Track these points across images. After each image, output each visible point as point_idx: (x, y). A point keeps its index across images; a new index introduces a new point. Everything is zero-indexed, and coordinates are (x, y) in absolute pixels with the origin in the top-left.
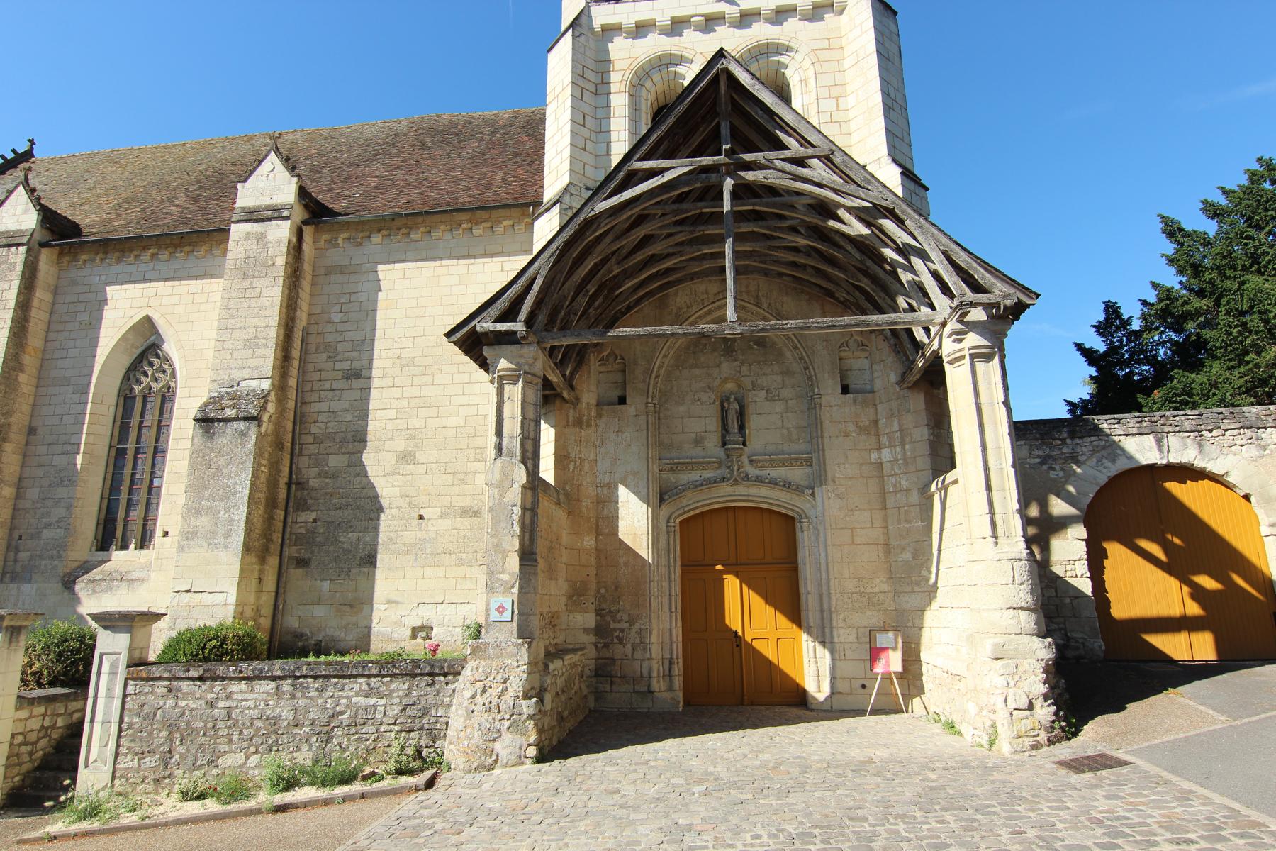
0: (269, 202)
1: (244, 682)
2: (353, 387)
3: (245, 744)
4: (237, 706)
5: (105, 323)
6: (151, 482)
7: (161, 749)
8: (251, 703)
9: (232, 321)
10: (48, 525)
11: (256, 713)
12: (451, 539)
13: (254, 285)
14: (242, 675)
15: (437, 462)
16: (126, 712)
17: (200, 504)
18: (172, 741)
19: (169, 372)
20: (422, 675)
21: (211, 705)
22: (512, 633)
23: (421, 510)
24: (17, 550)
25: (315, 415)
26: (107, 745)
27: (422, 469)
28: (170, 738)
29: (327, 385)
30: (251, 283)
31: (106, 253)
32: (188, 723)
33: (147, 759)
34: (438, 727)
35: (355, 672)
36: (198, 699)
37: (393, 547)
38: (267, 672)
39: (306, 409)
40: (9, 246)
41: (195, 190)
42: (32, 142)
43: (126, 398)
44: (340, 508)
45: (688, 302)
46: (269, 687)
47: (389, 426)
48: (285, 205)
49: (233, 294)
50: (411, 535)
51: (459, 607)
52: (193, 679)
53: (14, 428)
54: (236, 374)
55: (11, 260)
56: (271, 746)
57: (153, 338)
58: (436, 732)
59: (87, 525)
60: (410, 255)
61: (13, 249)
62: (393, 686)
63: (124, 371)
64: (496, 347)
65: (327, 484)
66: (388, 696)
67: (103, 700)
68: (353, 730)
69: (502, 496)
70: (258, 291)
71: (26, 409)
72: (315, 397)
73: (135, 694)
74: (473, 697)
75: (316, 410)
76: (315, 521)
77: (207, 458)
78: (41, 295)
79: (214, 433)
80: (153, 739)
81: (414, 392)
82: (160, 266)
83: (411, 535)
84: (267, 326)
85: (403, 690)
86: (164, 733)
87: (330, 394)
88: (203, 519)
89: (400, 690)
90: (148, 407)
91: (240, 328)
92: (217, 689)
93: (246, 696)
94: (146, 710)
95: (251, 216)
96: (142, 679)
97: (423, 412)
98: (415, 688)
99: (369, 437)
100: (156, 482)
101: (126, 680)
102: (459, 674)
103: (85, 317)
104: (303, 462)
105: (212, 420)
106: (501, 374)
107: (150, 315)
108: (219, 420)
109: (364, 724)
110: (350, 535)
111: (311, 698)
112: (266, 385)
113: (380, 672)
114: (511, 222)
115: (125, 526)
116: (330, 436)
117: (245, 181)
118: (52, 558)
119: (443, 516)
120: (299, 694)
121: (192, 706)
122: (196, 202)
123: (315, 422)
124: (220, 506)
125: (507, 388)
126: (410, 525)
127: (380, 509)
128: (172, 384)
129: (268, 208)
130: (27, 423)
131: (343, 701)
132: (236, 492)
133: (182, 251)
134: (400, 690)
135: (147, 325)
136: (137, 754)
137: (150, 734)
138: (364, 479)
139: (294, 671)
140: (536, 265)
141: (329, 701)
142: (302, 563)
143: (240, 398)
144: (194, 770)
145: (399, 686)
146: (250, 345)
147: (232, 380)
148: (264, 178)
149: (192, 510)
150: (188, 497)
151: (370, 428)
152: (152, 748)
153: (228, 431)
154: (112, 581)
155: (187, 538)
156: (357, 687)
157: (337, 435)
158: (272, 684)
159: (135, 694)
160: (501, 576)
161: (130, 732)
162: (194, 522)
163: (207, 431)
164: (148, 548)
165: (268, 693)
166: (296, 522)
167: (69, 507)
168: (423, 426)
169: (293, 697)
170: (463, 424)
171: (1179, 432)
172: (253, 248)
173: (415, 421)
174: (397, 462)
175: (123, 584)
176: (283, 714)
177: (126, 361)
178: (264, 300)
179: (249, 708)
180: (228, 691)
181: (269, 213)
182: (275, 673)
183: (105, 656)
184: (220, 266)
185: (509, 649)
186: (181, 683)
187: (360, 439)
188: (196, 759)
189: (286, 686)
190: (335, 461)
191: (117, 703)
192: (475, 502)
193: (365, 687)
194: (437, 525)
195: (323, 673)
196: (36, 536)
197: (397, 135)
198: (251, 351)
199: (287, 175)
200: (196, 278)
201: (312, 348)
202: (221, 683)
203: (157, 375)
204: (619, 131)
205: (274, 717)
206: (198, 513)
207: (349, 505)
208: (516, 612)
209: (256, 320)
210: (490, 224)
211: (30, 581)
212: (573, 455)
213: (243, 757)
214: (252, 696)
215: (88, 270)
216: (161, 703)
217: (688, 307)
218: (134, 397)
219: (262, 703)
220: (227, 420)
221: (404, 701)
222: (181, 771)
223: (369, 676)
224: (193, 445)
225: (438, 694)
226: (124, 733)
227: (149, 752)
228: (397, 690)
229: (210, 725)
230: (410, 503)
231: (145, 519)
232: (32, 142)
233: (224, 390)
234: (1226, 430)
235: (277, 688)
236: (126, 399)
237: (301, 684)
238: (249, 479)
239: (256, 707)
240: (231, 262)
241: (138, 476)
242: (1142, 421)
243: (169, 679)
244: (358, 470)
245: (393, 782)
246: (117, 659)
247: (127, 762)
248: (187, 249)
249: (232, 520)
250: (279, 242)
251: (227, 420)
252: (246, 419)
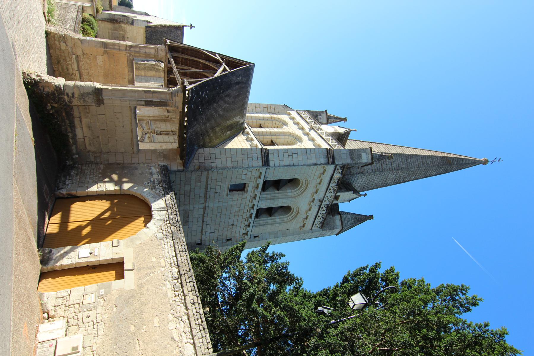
171: (168, 214)
234: (170, 228)
242: (173, 205)
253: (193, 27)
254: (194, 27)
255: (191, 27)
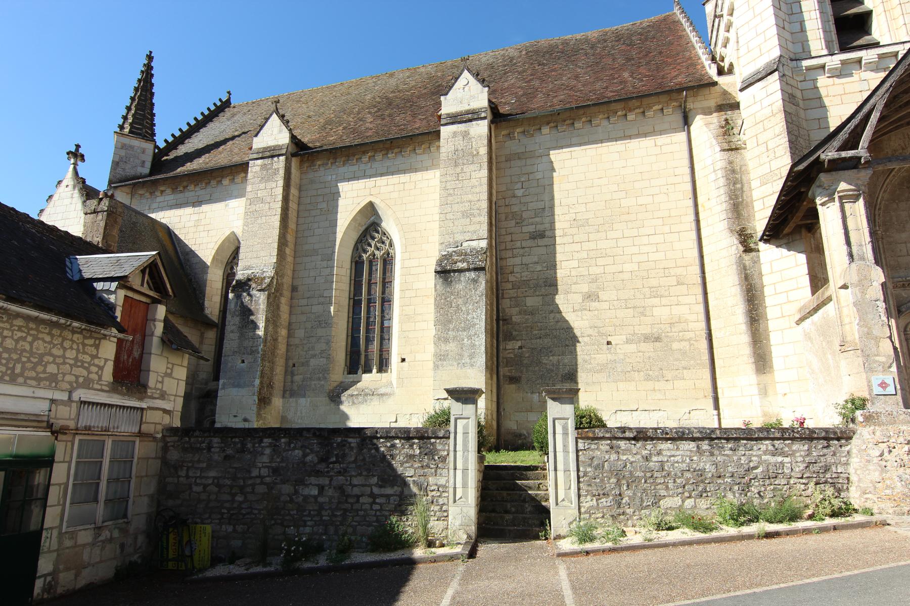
0: (467, 108)
1: (669, 442)
2: (539, 244)
3: (680, 490)
4: (668, 460)
5: (340, 209)
6: (382, 323)
7: (613, 492)
8: (678, 458)
9: (450, 198)
10: (314, 356)
11: (684, 466)
12: (638, 359)
13: (465, 170)
14: (668, 436)
15: (618, 300)
16: (580, 463)
17: (447, 334)
18: (620, 486)
19: (387, 243)
20: (818, 439)
21: (647, 459)
22: (898, 404)
23: (609, 337)
24: (293, 374)
25: (511, 268)
26: (570, 488)
27: (605, 305)
28: (618, 484)
29: (518, 244)
30: (462, 169)
31: (335, 158)
32: (631, 472)
33: (602, 500)
34: (841, 482)
35: (761, 435)
36: (635, 454)
37: (589, 366)
38: (688, 434)
39: (504, 263)
40: (272, 157)
41: (376, 112)
42: (229, 93)
43: (356, 263)
44: (540, 338)
45: (903, 144)
46: (691, 446)
47: (574, 273)
48: (481, 109)
49: (449, 178)
50: (603, 357)
51: (652, 414)
52: (629, 439)
53: (285, 286)
54: (459, 237)
55: (275, 166)
56: (702, 492)
57: (373, 218)
58: (840, 485)
59: (340, 355)
60: (574, 140)
61: (276, 159)
62: (795, 447)
63: (354, 243)
64: (834, 173)
65: (527, 319)
66: (793, 454)
67: (562, 454)
68: (767, 482)
69: (863, 293)
70: (468, 174)
71: (290, 273)
72: (509, 254)
73: (585, 450)
74: (882, 455)
75: (511, 263)
76: (520, 348)
77: (448, 299)
78: (294, 191)
79: (451, 281)
80: (605, 484)
81: (592, 245)
82: (376, 165)
83: (603, 357)
84: (479, 200)
85: (803, 451)
86: (613, 480)
87: (521, 251)
88: (451, 345)
89: (801, 451)
90: (374, 268)
91: (458, 203)
92: (649, 447)
93: (673, 453)
94: (595, 462)
95: (456, 119)
96: (588, 438)
97: (600, 262)
98: (814, 450)
99: (559, 283)
100: (386, 324)
101: (577, 438)
102: (851, 438)
103: (324, 205)
104: (506, 303)
105: (449, 272)
106: (841, 194)
107: (373, 200)
108: (454, 271)
109: (776, 477)
110: (551, 358)
111: (727, 455)
112: (484, 244)
113: (783, 435)
114: (660, 107)
115: (366, 356)
116: (525, 283)
117: (446, 94)
118: (319, 379)
119: (628, 341)
120: (716, 452)
121: (632, 460)
122: (383, 119)
123: (511, 273)
124: (463, 335)
125: (847, 206)
126: (601, 349)
127: (574, 340)
128: (391, 251)
129: (468, 112)
130: (291, 284)
131: (753, 458)
132: (474, 325)
133: (392, 153)
134: (801, 451)
135: (370, 209)
136: (594, 496)
137: (602, 480)
138: (557, 315)
139: (710, 434)
140: (872, 101)
141: (742, 458)
142: (513, 380)
143: (466, 254)
144: (642, 509)
145: (800, 448)
146: (466, 215)
147: (457, 242)
148: (461, 90)
149: (441, 339)
150: (437, 329)
151: (559, 275)
152: (605, 491)
153: (462, 279)
154: (366, 395)
155: (440, 359)
156: (763, 448)
157: (531, 282)
158: (692, 445)
159: (585, 450)
160: (877, 358)
161: (586, 479)
162: (443, 347)
163: (446, 280)
164: (386, 371)
165: (691, 451)
166: (505, 349)
167: (328, 343)
168: (602, 272)
169: (712, 454)
170: (637, 269)
172: (460, 143)
173: (595, 268)
174: (583, 301)
175: (375, 398)
176: (706, 468)
177: (355, 236)
178: (474, 181)
179: (677, 462)
180: (658, 448)
181: (470, 116)
182: (695, 435)
183: (556, 421)
184: (422, 161)
185: (901, 417)
186: (619, 442)
187: (552, 285)
188: (642, 501)
189: (705, 445)
190: (531, 302)
191: (572, 456)
192: (655, 330)
193: (770, 448)
194: (624, 349)
195: (735, 436)
196: (306, 364)
197: (512, 59)
198: (468, 220)
199: (479, 86)
200: (404, 172)
201: (503, 217)
202: (651, 442)
203: (379, 245)
204: (810, 11)
205: (699, 469)
206: (446, 340)
207: (547, 335)
208: (898, 387)
209: (470, 196)
210: (642, 110)
211: (304, 396)
212: (818, 275)
213: (680, 500)
214: (678, 453)
215: (324, 173)
216: (607, 457)
217: (903, 149)
218: (363, 262)
219: (688, 459)
220: (461, 271)
221: (807, 459)
222: (632, 510)
223: (773, 439)
224: (436, 291)
225: (834, 454)
226: (581, 480)
227: (604, 494)
228: (799, 451)
229: (649, 475)
230: (599, 332)
231: (381, 350)
232: (229, 93)
233: (451, 250)
235: (698, 447)
236: (357, 264)
237: (717, 444)
238: (484, 314)
239: (683, 462)
240: (444, 155)
241: (372, 320)
243: (610, 439)
244: (551, 308)
245: (789, 527)
246: (567, 423)
247: (588, 502)
248: (396, 150)
249: (474, 345)
250: (480, 137)
251: (461, 271)
252: (476, 269)
253: (77, 150)
254: (78, 146)
255: (76, 155)
